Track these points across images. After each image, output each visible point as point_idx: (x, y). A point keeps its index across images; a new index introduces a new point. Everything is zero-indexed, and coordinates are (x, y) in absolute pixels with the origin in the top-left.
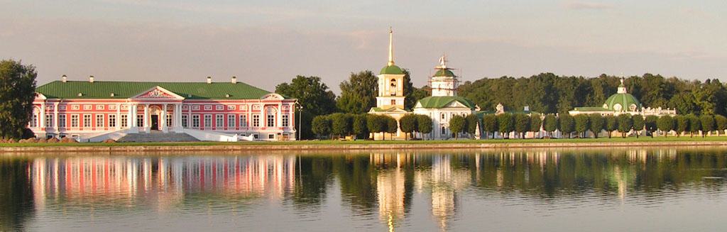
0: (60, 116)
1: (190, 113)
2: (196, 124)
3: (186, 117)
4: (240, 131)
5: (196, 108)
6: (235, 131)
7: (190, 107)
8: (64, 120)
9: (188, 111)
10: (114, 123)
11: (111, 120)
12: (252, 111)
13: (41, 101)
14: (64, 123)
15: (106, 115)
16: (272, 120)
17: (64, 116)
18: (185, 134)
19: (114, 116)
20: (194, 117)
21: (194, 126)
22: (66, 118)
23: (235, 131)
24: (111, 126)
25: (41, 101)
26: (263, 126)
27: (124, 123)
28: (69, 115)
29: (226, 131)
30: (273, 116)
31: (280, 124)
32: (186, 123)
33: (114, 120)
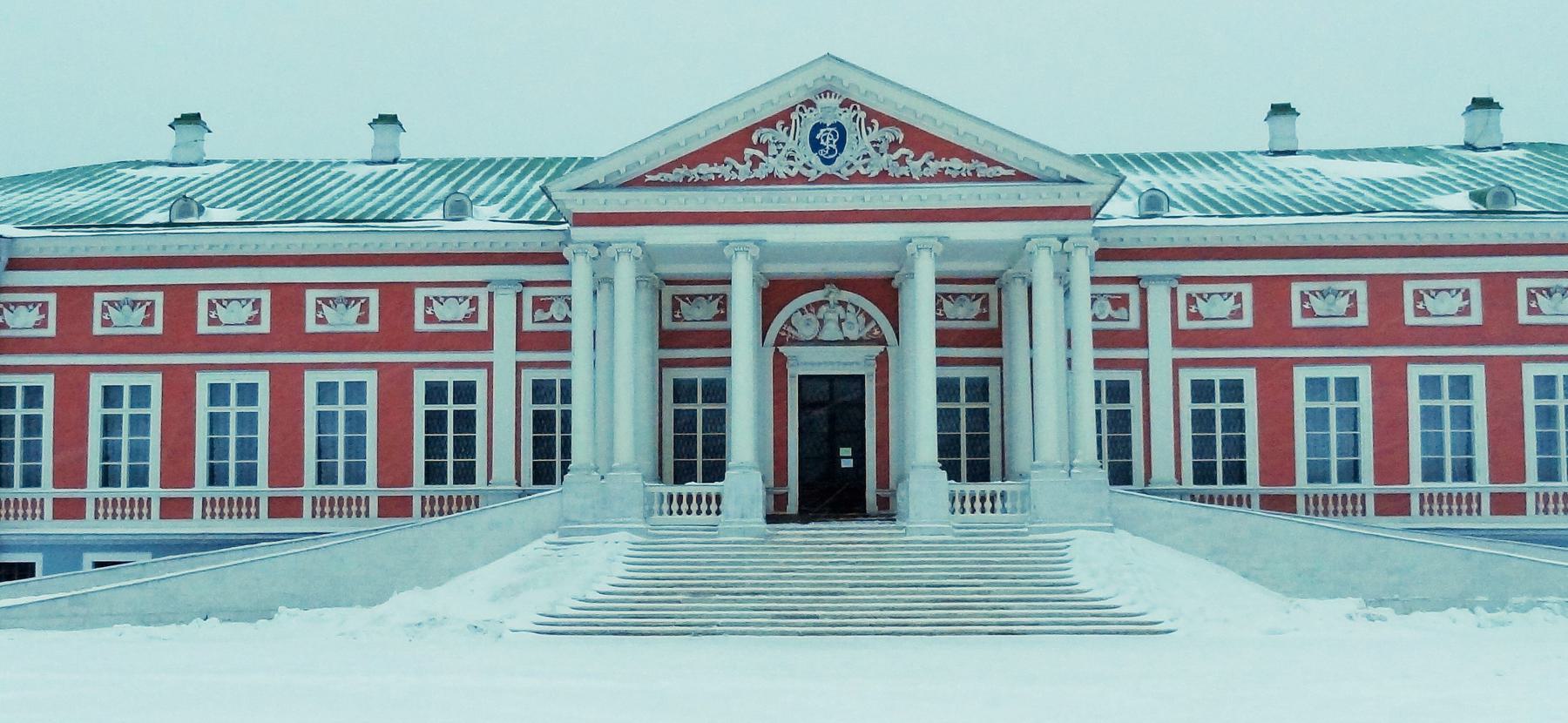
1: (1161, 351)
5: (1217, 311)
7: (1159, 299)
10: (465, 447)
20: (1202, 391)
21: (1204, 474)
33: (466, 421)
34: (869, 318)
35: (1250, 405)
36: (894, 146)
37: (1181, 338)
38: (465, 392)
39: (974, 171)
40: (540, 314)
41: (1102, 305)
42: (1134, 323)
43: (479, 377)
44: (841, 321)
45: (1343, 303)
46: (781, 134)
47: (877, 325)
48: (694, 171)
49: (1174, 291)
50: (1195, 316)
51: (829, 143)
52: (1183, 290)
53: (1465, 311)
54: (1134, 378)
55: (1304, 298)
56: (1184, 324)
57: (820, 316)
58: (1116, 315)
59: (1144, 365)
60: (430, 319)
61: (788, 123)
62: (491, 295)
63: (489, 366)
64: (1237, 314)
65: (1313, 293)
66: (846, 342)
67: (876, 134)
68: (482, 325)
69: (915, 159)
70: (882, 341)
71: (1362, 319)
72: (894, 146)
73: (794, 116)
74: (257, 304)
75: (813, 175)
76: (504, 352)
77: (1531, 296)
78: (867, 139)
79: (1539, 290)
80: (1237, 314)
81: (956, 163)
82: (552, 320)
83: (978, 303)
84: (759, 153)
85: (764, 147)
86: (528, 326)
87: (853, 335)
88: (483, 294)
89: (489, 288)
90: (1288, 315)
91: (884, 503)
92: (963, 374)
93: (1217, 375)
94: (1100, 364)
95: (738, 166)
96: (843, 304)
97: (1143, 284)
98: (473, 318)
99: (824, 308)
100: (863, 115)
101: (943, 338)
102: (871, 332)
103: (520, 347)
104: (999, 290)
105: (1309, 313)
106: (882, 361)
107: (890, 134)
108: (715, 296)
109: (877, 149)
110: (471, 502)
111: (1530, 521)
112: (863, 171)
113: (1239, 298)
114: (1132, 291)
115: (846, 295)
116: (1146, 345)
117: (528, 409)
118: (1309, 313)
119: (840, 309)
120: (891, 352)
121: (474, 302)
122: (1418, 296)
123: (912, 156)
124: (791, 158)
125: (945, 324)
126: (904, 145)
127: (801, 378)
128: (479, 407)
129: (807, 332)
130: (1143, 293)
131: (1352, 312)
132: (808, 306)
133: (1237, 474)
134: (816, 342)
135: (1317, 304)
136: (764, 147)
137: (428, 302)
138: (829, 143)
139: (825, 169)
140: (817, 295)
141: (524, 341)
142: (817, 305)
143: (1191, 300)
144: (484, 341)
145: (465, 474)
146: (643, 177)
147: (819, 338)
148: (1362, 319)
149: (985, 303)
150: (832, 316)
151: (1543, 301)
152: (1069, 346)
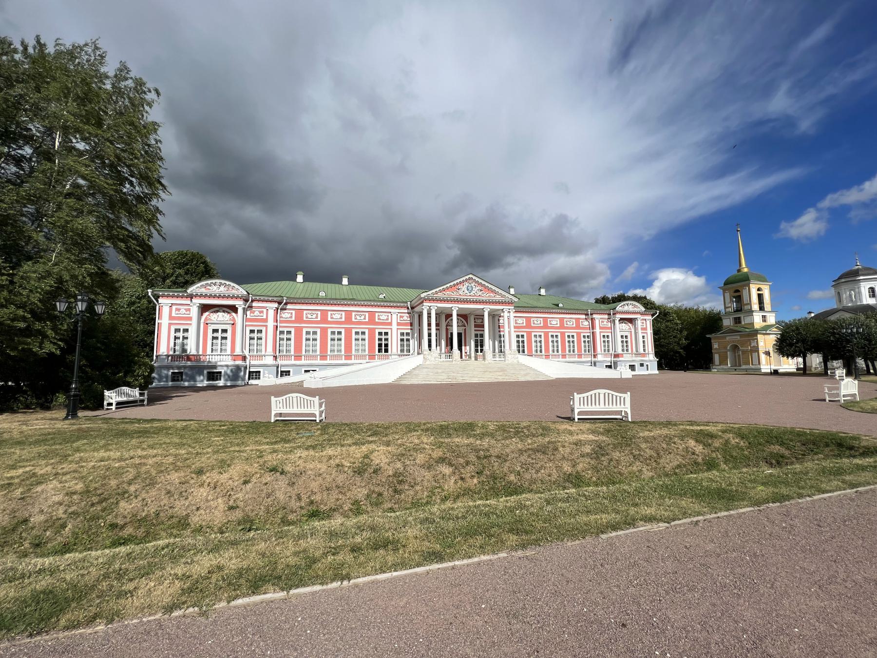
6: (576, 359)
11: (380, 340)
12: (601, 328)
13: (237, 298)
15: (372, 331)
19: (386, 334)
20: (518, 336)
23: (576, 359)
24: (380, 351)
35: (525, 339)
38: (386, 334)
51: (470, 289)
63: (391, 329)
68: (390, 321)
71: (542, 325)
76: (394, 326)
86: (399, 321)
93: (520, 334)
94: (515, 331)
103: (398, 325)
106: (465, 329)
110: (387, 357)
111: (567, 359)
122: (550, 321)
131: (573, 324)
133: (523, 351)
135: (535, 322)
138: (470, 289)
141: (398, 324)
144: (390, 324)
145: (386, 351)
148: (542, 325)
151: (568, 323)
152: (419, 326)
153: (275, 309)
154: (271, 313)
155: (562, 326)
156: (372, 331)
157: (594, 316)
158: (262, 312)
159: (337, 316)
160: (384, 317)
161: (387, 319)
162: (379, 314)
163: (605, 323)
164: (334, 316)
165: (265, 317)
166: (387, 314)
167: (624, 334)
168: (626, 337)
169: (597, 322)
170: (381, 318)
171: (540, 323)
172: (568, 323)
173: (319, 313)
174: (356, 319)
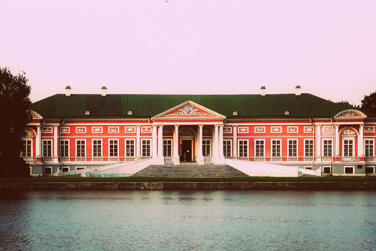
0: (60, 143)
1: (235, 137)
2: (243, 153)
3: (229, 142)
4: (304, 162)
5: (243, 130)
7: (235, 129)
8: (67, 147)
9: (232, 135)
14: (67, 151)
16: (351, 146)
17: (67, 142)
18: (227, 166)
19: (132, 142)
22: (69, 145)
25: (37, 121)
26: (337, 153)
27: (146, 151)
28: (72, 140)
29: (284, 162)
30: (351, 142)
31: (361, 152)
32: (229, 151)
34: (192, 131)
36: (197, 112)
37: (238, 135)
38: (132, 142)
39: (208, 115)
40: (143, 130)
41: (226, 130)
42: (231, 132)
43: (134, 140)
44: (188, 132)
45: (262, 130)
46: (182, 110)
47: (194, 133)
48: (171, 115)
49: (237, 128)
50: (240, 131)
52: (239, 128)
53: (279, 131)
54: (231, 141)
55: (256, 129)
56: (239, 132)
57: (185, 131)
58: (229, 131)
59: (232, 139)
60: (127, 131)
61: (183, 108)
62: (136, 127)
64: (246, 131)
65: (257, 128)
66: (189, 135)
67: (195, 110)
68: (135, 132)
69: (200, 113)
70: (194, 135)
71: (265, 132)
72: (197, 112)
73: (184, 108)
74: (101, 128)
75: (186, 115)
76: (138, 136)
77: (289, 129)
78: (193, 111)
79: (290, 128)
80: (246, 131)
81: (205, 114)
82: (145, 131)
83: (209, 129)
84: (180, 113)
85: (180, 112)
86: (142, 132)
87: (190, 134)
88: (135, 127)
89: (136, 126)
90: (254, 131)
91: (194, 159)
92: (206, 140)
95: (177, 114)
96: (189, 129)
97: (233, 127)
98: (133, 131)
99: (186, 130)
100: (193, 107)
101: (203, 135)
102: (193, 133)
104: (212, 127)
105: (257, 131)
107: (196, 110)
108: (170, 128)
109: (195, 112)
112: (193, 115)
113: (247, 129)
114: (231, 128)
115: (189, 128)
116: (233, 136)
117: (142, 144)
118: (257, 131)
119: (188, 130)
120: (195, 137)
121: (133, 128)
123: (199, 113)
124: (183, 113)
125: (204, 132)
126: (199, 111)
127: (183, 141)
128: (135, 144)
129: (183, 133)
130: (233, 128)
132: (183, 130)
134: (184, 135)
135: (258, 130)
136: (180, 112)
137: (127, 128)
139: (188, 115)
140: (185, 128)
141: (141, 134)
142: (185, 129)
143: (240, 129)
144: (135, 134)
145: (132, 155)
146: (164, 115)
147: (185, 134)
149: (209, 129)
150: (187, 131)
151: (291, 130)
153: (58, 126)
154: (56, 129)
155: (285, 133)
156: (122, 140)
157: (316, 124)
158: (50, 129)
159: (97, 130)
160: (130, 129)
161: (133, 131)
162: (127, 127)
163: (328, 129)
164: (96, 130)
165: (52, 132)
166: (133, 127)
167: (349, 139)
168: (351, 142)
169: (318, 128)
170: (129, 130)
171: (263, 131)
172: (291, 130)
173: (86, 127)
174: (111, 131)
